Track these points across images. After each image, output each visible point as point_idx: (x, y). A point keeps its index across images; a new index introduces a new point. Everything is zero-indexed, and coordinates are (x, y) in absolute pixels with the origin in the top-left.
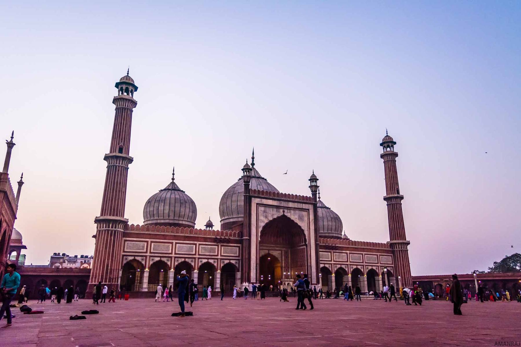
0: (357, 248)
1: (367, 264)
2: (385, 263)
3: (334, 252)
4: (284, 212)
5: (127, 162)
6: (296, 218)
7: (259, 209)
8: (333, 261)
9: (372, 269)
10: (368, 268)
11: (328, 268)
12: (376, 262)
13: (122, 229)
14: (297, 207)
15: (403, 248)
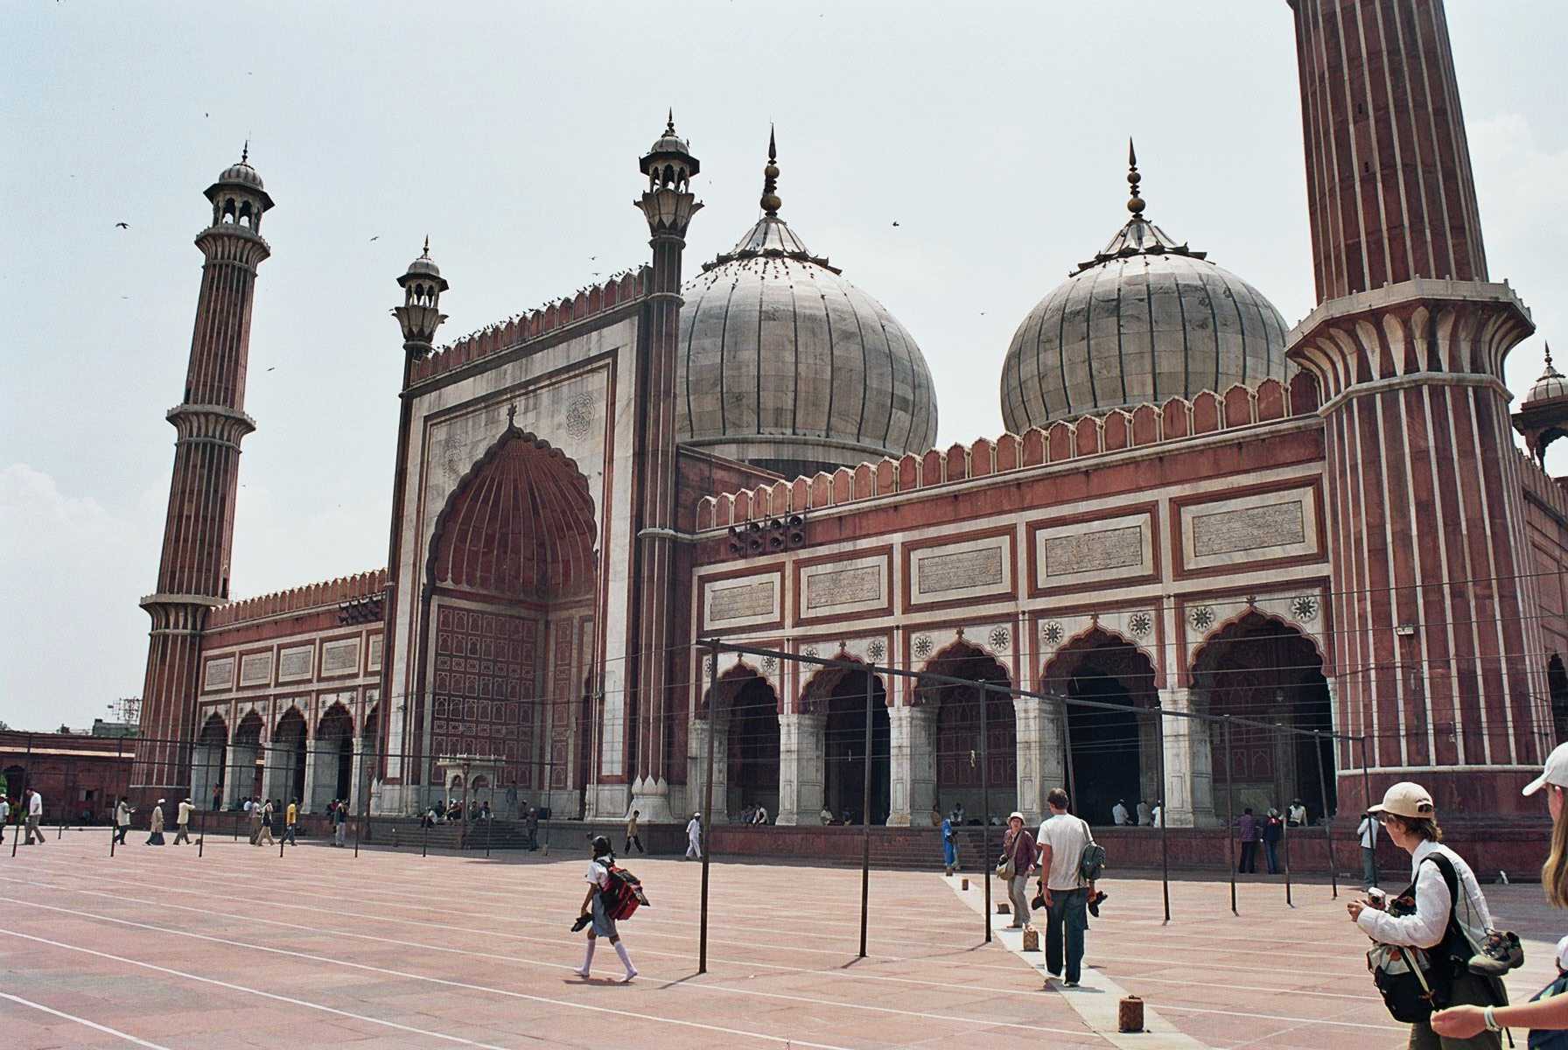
0: (969, 494)
1: (1041, 603)
2: (1239, 558)
3: (799, 565)
4: (512, 413)
5: (203, 419)
6: (559, 426)
7: (433, 440)
8: (788, 621)
9: (1096, 633)
10: (1053, 634)
11: (761, 670)
12: (1136, 572)
13: (185, 627)
14: (562, 364)
15: (1354, 380)
